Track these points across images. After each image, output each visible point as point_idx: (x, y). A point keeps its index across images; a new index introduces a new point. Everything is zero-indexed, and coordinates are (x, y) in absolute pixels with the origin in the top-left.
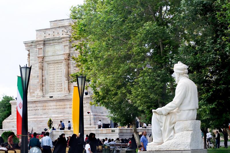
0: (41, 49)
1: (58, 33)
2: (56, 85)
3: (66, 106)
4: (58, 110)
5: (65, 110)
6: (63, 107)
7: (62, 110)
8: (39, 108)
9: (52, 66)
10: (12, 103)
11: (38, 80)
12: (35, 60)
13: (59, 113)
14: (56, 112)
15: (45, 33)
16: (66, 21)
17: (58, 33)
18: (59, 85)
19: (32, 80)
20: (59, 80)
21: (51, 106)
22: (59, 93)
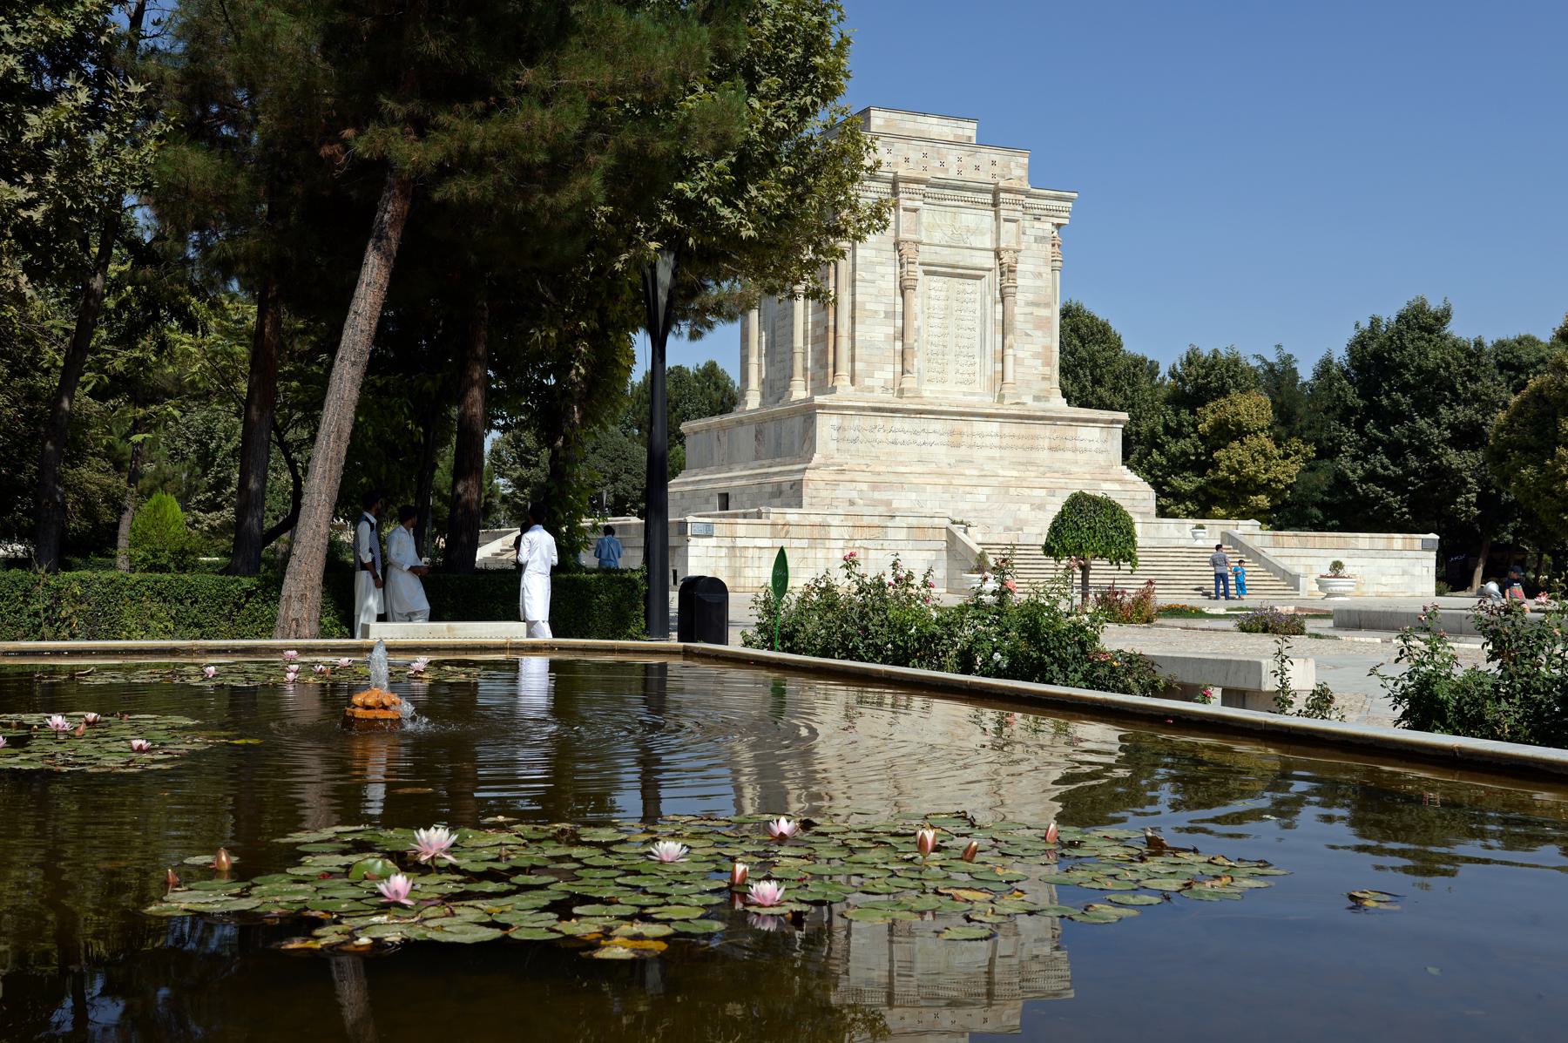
0: (915, 210)
1: (942, 164)
2: (951, 357)
3: (1036, 443)
4: (1007, 453)
5: (1035, 455)
6: (1028, 443)
7: (1022, 455)
8: (932, 438)
9: (937, 283)
10: (822, 407)
11: (891, 331)
12: (879, 250)
13: (1012, 463)
14: (1002, 458)
15: (889, 152)
16: (934, 120)
17: (942, 164)
18: (962, 360)
19: (863, 323)
20: (965, 342)
21: (981, 435)
22: (965, 388)
